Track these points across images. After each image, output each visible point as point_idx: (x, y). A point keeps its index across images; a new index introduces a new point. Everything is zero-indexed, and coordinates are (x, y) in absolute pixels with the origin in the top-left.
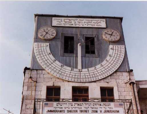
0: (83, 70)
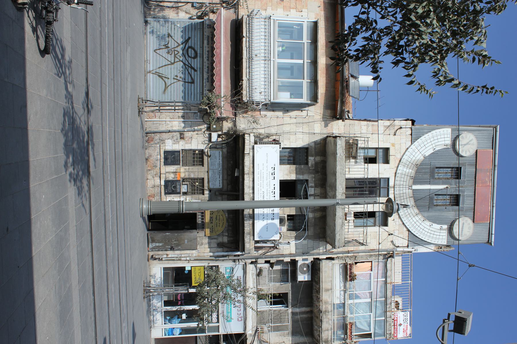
0: (410, 191)
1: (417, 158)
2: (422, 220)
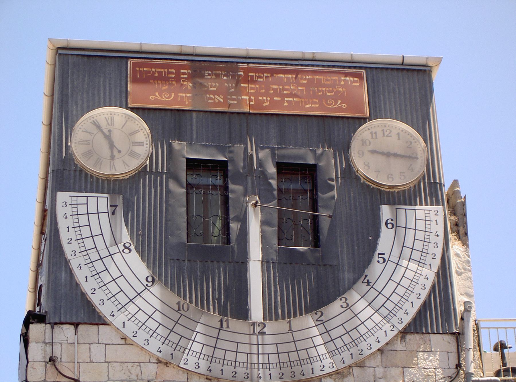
0: (271, 327)
1: (157, 304)
2: (365, 288)
